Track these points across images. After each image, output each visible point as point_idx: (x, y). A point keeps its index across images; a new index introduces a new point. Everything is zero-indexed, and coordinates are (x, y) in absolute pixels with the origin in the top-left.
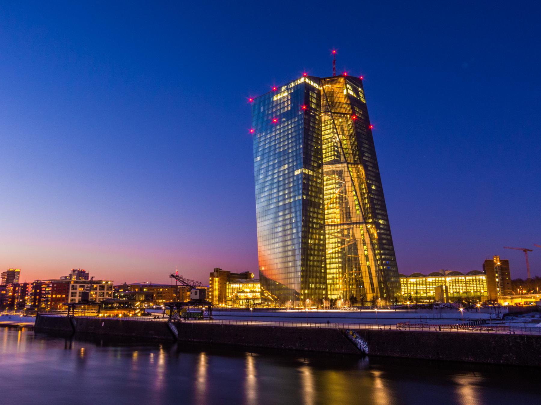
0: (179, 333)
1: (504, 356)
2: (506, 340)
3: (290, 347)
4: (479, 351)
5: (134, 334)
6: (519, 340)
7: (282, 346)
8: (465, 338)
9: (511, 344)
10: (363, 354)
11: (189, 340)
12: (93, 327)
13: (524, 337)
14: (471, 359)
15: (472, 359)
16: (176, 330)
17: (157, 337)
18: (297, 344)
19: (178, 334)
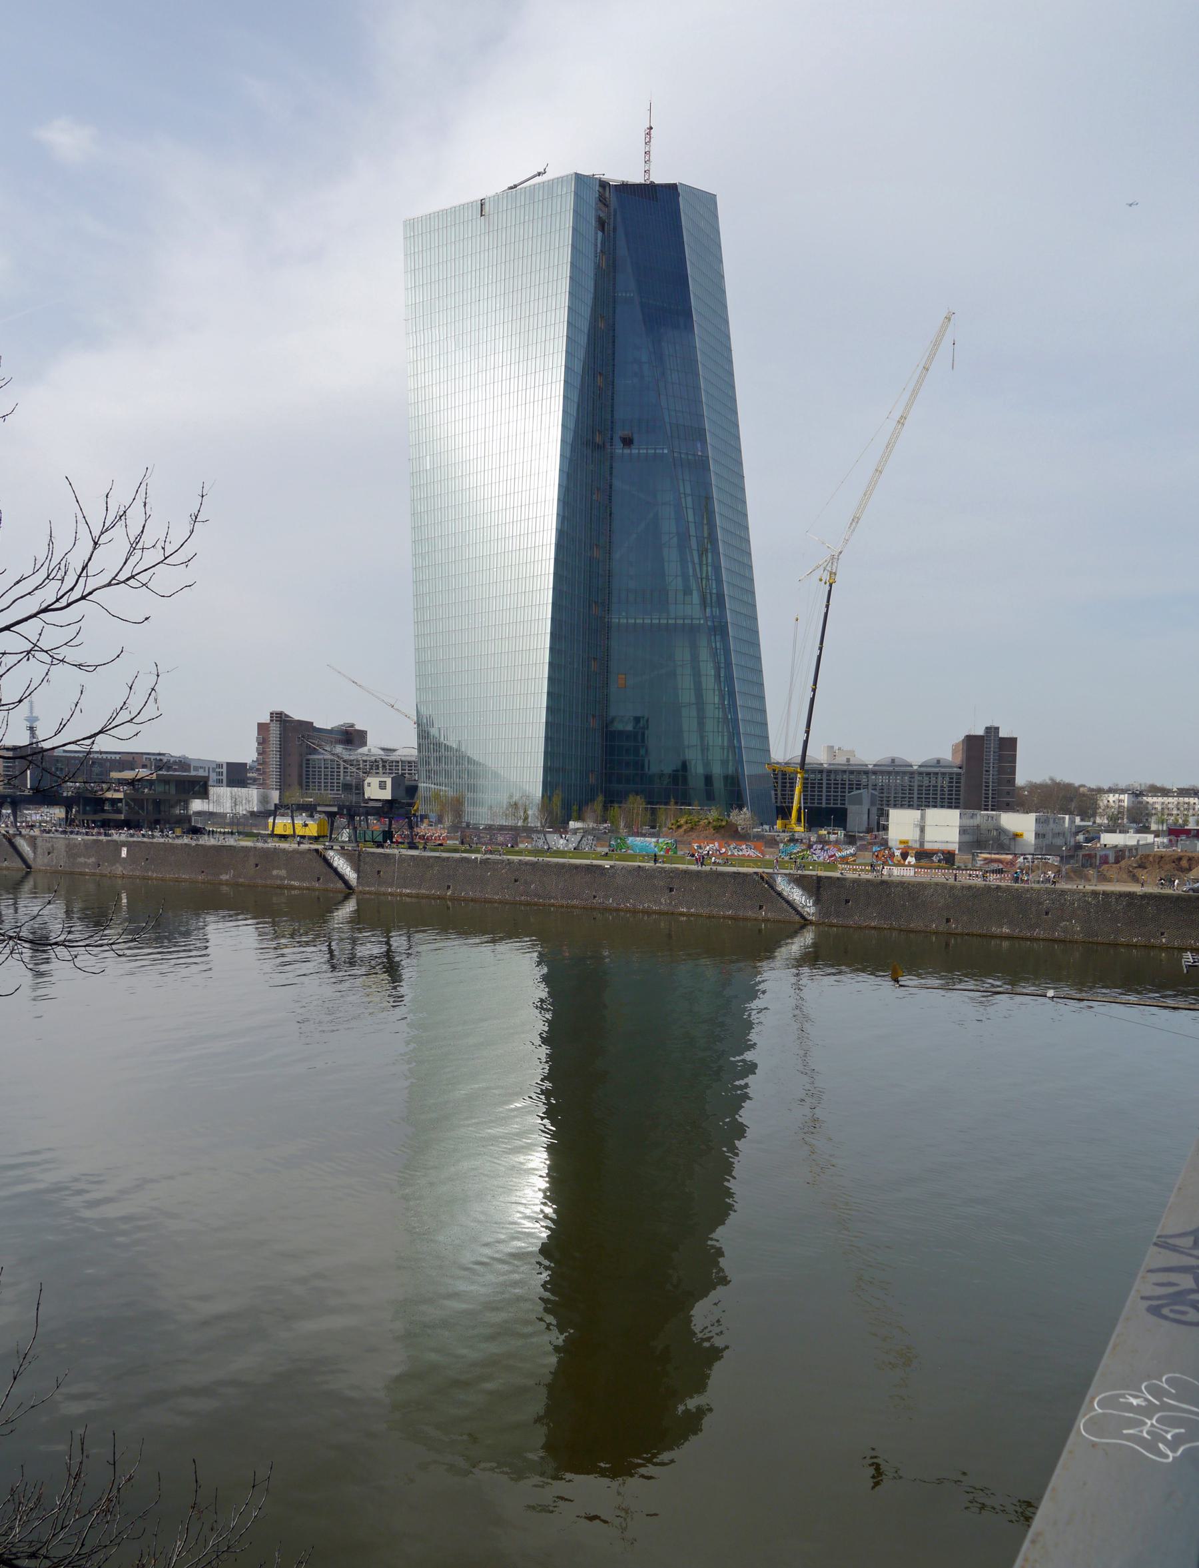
0: (358, 875)
1: (1061, 925)
3: (646, 905)
4: (1021, 916)
5: (224, 877)
6: (1090, 899)
7: (628, 905)
8: (999, 894)
9: (1076, 905)
10: (805, 923)
11: (390, 890)
12: (92, 860)
13: (1099, 894)
14: (1006, 930)
15: (1007, 931)
16: (349, 869)
17: (296, 883)
19: (359, 878)
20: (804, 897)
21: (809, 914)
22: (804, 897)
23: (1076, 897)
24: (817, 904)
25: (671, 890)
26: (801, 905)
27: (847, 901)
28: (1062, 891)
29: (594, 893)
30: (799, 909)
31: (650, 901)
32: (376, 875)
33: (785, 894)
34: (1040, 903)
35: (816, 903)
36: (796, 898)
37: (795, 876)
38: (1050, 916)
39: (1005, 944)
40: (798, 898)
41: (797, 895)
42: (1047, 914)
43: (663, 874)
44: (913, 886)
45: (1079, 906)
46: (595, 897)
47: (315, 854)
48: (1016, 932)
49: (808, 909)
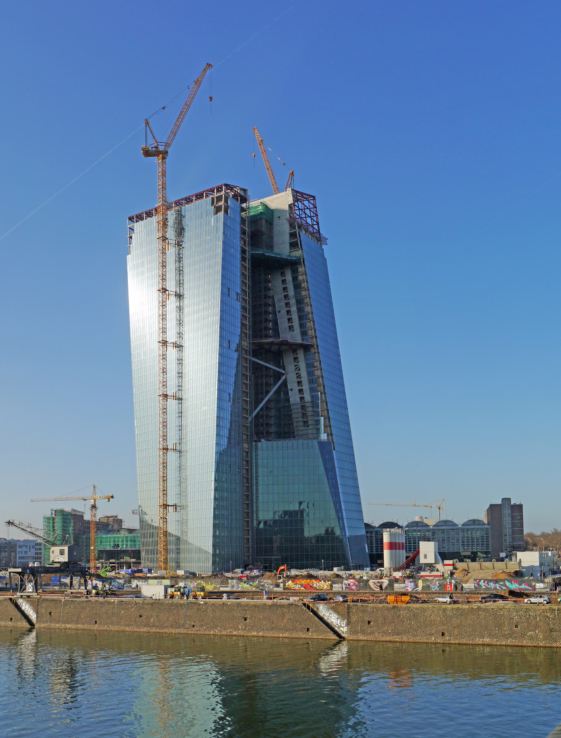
2: (532, 614)
9: (538, 619)
14: (487, 640)
18: (240, 627)
20: (339, 620)
21: (343, 632)
22: (339, 620)
23: (538, 613)
24: (348, 625)
25: (246, 619)
26: (337, 626)
27: (369, 622)
28: (527, 609)
29: (193, 623)
30: (336, 629)
31: (231, 628)
32: (49, 616)
33: (326, 618)
34: (512, 619)
35: (348, 624)
36: (333, 620)
37: (332, 605)
38: (519, 628)
39: (487, 649)
40: (334, 621)
41: (333, 619)
42: (516, 627)
43: (240, 608)
44: (416, 609)
45: (540, 620)
46: (194, 626)
47: (9, 602)
48: (494, 641)
49: (342, 629)
